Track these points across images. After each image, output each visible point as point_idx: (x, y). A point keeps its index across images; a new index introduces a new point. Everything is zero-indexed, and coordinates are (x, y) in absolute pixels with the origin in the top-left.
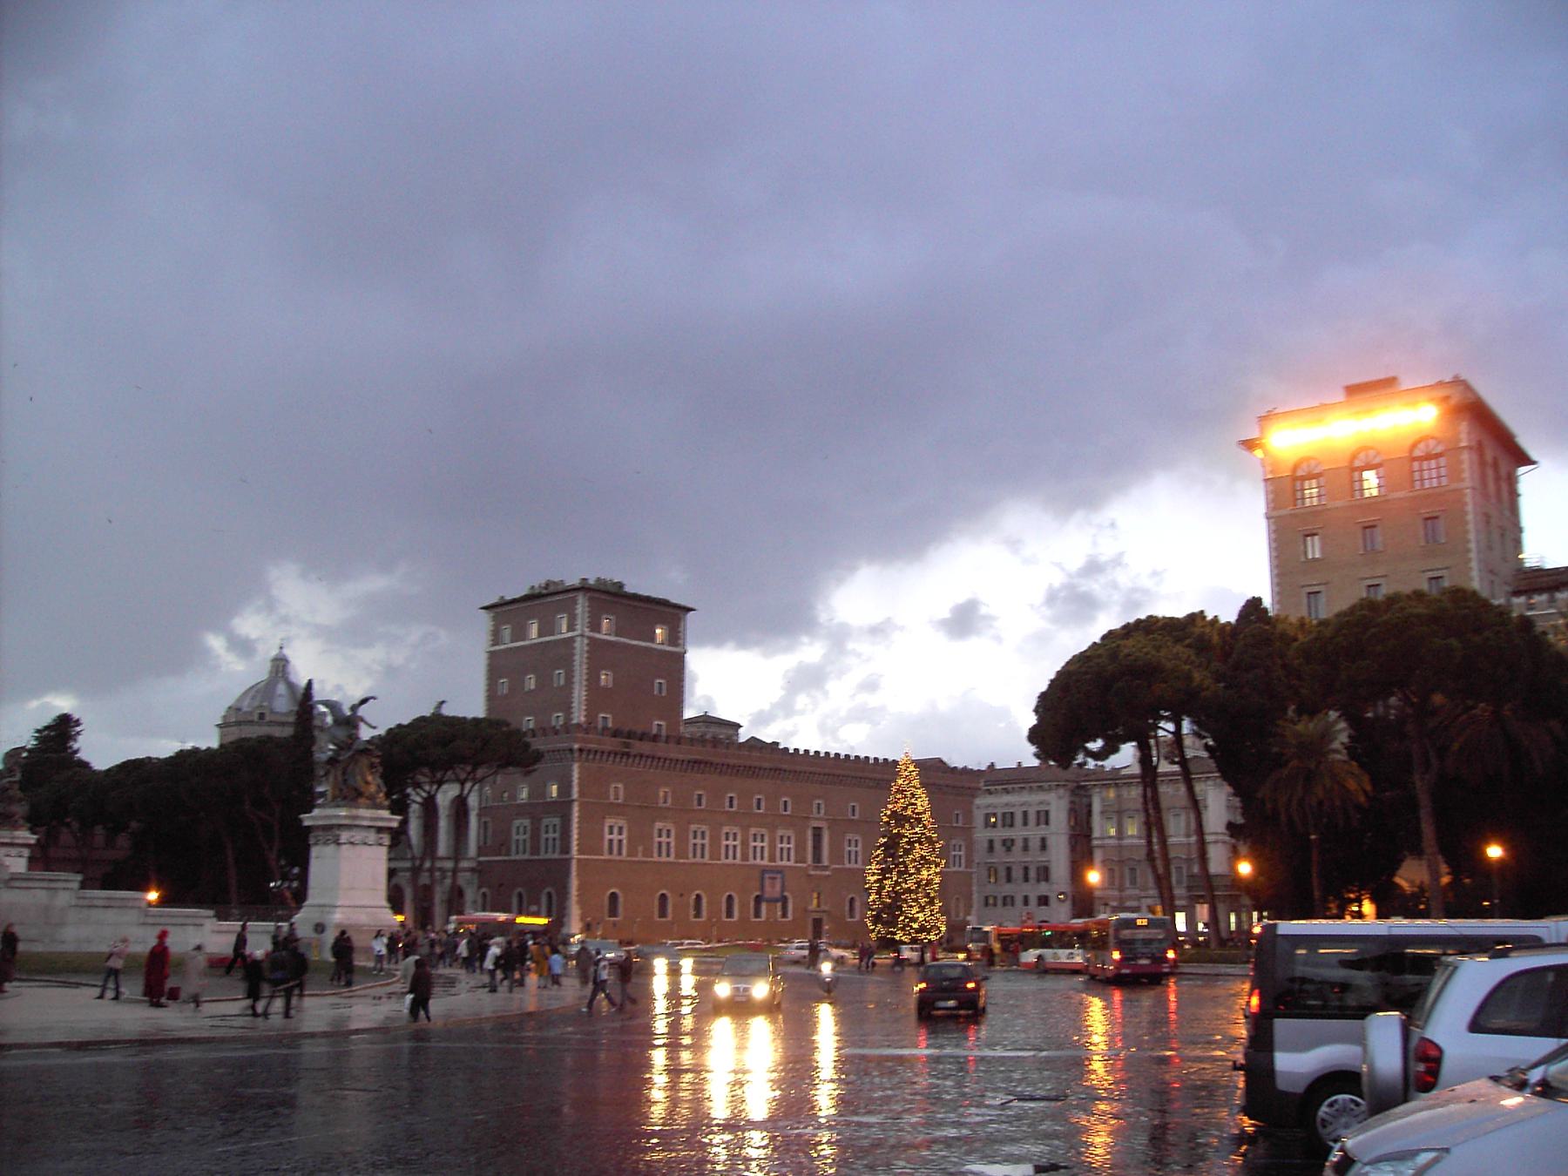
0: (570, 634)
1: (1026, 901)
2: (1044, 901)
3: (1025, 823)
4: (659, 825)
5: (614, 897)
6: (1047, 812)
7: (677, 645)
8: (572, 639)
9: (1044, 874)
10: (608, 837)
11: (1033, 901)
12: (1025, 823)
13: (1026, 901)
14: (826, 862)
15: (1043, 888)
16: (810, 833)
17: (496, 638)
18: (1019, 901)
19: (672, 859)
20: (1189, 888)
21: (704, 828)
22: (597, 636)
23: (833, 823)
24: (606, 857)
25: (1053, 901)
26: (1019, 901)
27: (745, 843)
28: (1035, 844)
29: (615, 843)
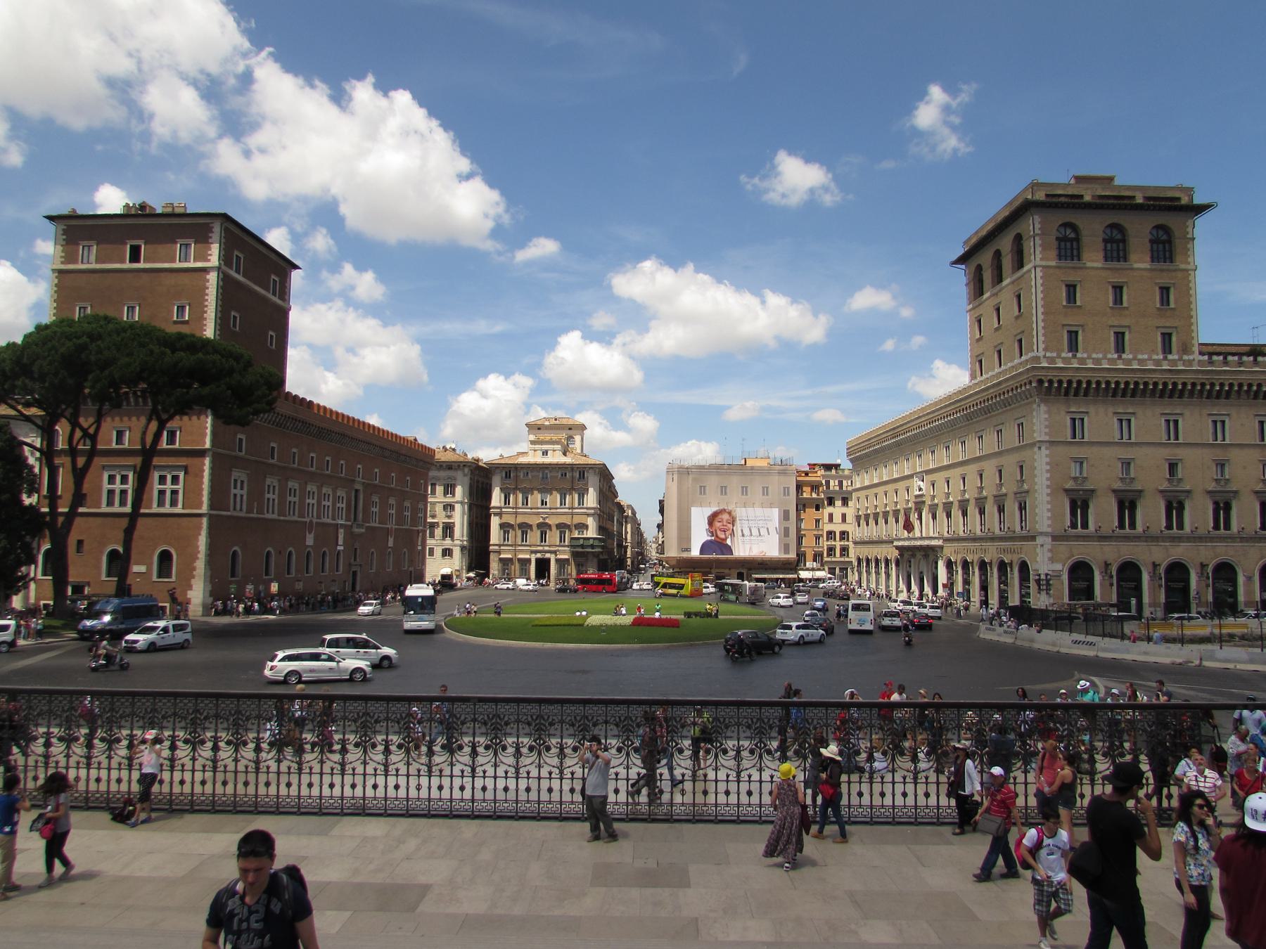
0: (199, 265)
2: (447, 553)
8: (205, 270)
9: (448, 529)
10: (233, 491)
15: (448, 541)
17: (70, 257)
23: (366, 486)
27: (319, 502)
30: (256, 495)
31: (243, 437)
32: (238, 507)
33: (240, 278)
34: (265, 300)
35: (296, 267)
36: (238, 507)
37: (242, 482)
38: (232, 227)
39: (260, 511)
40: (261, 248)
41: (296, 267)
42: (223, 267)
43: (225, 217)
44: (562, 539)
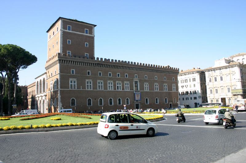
1: (191, 98)
2: (195, 98)
3: (190, 81)
4: (87, 80)
5: (73, 100)
6: (195, 78)
7: (92, 34)
11: (193, 98)
12: (190, 81)
13: (191, 98)
14: (139, 89)
16: (134, 83)
18: (190, 99)
19: (92, 89)
20: (232, 93)
21: (102, 81)
22: (66, 30)
23: (140, 81)
24: (70, 89)
25: (198, 98)
26: (190, 99)
28: (193, 86)
29: (73, 85)
30: (81, 83)
31: (74, 70)
32: (73, 88)
33: (71, 31)
34: (82, 35)
35: (95, 26)
36: (73, 88)
37: (157, 85)
38: (63, 20)
39: (84, 88)
40: (79, 23)
41: (95, 26)
42: (62, 29)
43: (60, 18)
44: (229, 91)
